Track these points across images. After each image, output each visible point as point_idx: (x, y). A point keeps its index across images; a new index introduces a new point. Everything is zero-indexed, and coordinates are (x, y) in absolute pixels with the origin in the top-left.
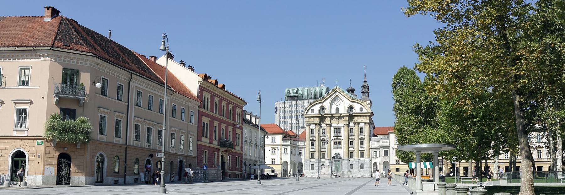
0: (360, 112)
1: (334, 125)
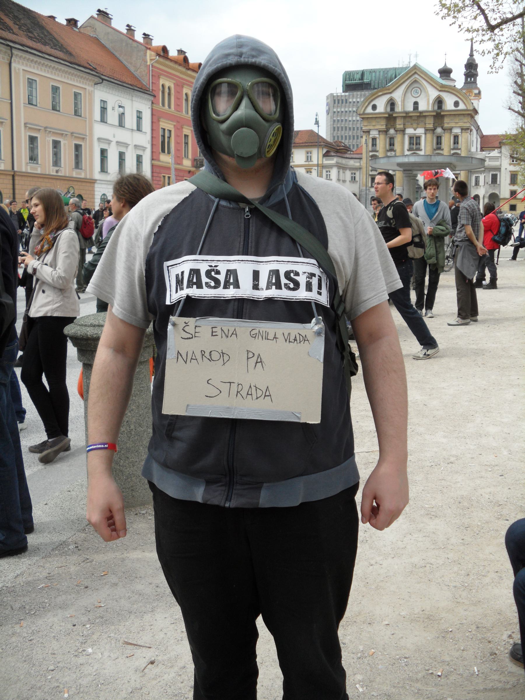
0: (453, 108)
1: (410, 131)
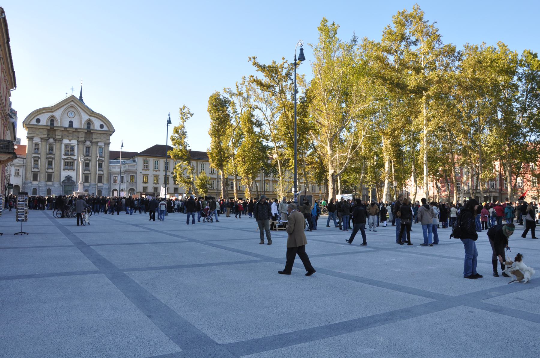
0: (100, 129)
